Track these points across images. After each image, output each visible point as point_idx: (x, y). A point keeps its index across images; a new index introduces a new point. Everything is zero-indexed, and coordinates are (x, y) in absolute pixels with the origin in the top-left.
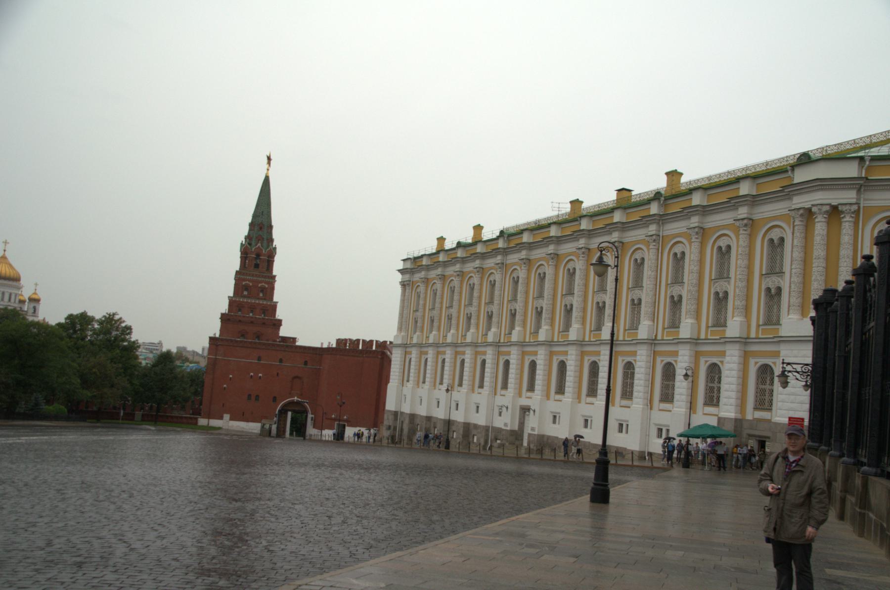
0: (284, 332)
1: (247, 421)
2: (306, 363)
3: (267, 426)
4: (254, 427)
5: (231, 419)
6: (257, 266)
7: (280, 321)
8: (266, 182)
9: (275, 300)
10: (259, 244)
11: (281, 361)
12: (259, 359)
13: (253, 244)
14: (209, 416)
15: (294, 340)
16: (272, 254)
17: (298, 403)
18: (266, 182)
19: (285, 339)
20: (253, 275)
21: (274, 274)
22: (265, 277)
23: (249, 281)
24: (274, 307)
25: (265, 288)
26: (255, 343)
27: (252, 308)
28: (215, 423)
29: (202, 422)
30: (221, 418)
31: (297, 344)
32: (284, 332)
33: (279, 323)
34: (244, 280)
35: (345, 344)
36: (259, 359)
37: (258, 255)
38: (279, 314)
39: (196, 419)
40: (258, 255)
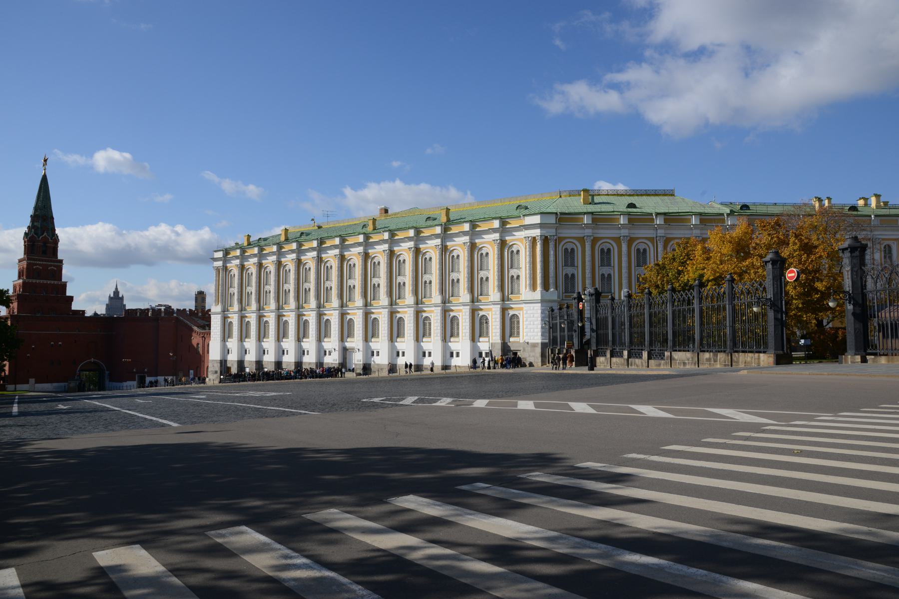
0: (75, 306)
5: (36, 382)
7: (71, 299)
8: (44, 180)
15: (84, 312)
17: (94, 363)
18: (44, 180)
21: (60, 257)
22: (51, 261)
24: (64, 286)
30: (28, 382)
32: (75, 306)
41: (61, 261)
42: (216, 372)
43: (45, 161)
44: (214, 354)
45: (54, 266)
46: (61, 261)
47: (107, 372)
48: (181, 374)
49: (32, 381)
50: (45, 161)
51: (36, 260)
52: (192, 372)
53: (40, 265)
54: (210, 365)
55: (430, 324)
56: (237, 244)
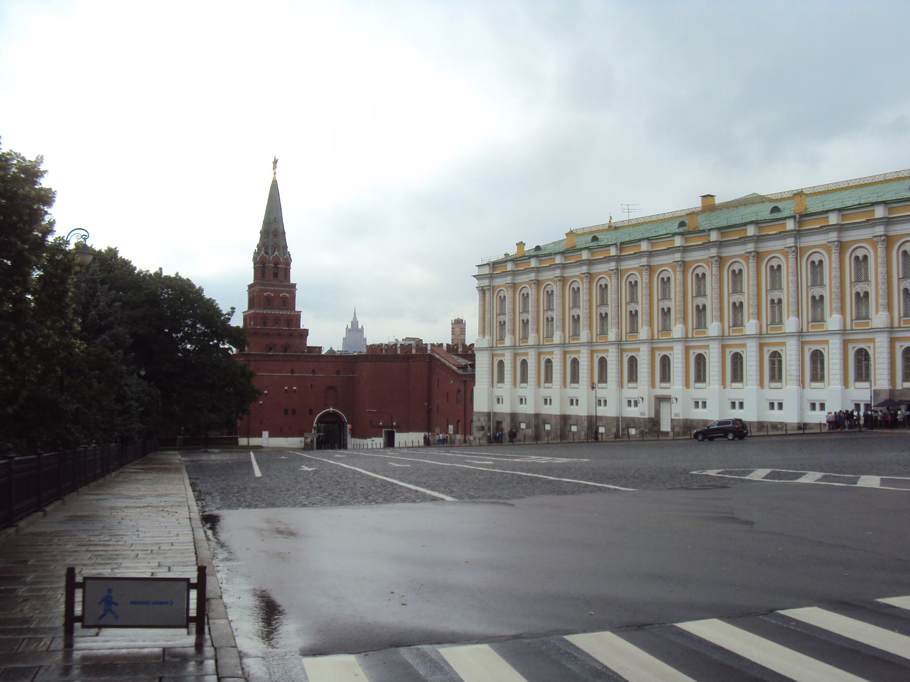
0: (311, 342)
1: (286, 436)
2: (338, 372)
3: (309, 440)
4: (295, 442)
5: (271, 436)
6: (276, 275)
7: (305, 333)
8: (274, 188)
9: (297, 309)
10: (276, 253)
11: (313, 372)
12: (292, 371)
13: (270, 252)
14: (248, 435)
15: (320, 348)
16: (288, 261)
17: (334, 413)
18: (274, 188)
19: (311, 349)
20: (274, 286)
21: (292, 281)
22: (283, 286)
23: (271, 291)
24: (297, 317)
25: (287, 298)
26: (287, 356)
27: (277, 319)
28: (254, 441)
29: (243, 441)
30: (260, 436)
31: (323, 353)
32: (311, 342)
33: (305, 333)
34: (267, 291)
35: (382, 350)
36: (292, 371)
37: (276, 264)
38: (304, 325)
39: (237, 438)
40: (276, 264)
41: (294, 286)
42: (482, 428)
43: (275, 162)
44: (481, 402)
45: (287, 292)
46: (294, 286)
47: (349, 426)
48: (437, 430)
49: (265, 434)
50: (275, 162)
51: (268, 285)
52: (451, 427)
53: (271, 291)
54: (475, 418)
55: (780, 362)
56: (506, 255)
